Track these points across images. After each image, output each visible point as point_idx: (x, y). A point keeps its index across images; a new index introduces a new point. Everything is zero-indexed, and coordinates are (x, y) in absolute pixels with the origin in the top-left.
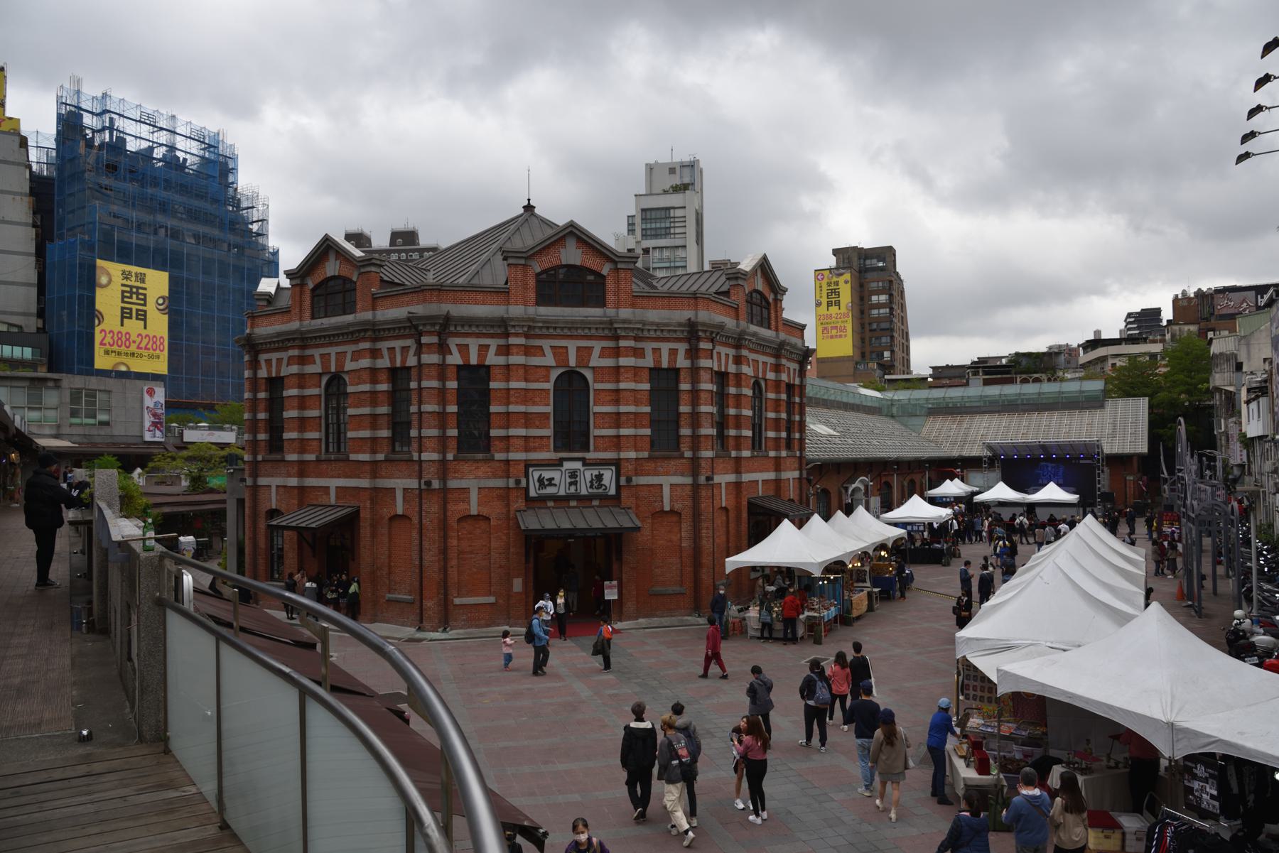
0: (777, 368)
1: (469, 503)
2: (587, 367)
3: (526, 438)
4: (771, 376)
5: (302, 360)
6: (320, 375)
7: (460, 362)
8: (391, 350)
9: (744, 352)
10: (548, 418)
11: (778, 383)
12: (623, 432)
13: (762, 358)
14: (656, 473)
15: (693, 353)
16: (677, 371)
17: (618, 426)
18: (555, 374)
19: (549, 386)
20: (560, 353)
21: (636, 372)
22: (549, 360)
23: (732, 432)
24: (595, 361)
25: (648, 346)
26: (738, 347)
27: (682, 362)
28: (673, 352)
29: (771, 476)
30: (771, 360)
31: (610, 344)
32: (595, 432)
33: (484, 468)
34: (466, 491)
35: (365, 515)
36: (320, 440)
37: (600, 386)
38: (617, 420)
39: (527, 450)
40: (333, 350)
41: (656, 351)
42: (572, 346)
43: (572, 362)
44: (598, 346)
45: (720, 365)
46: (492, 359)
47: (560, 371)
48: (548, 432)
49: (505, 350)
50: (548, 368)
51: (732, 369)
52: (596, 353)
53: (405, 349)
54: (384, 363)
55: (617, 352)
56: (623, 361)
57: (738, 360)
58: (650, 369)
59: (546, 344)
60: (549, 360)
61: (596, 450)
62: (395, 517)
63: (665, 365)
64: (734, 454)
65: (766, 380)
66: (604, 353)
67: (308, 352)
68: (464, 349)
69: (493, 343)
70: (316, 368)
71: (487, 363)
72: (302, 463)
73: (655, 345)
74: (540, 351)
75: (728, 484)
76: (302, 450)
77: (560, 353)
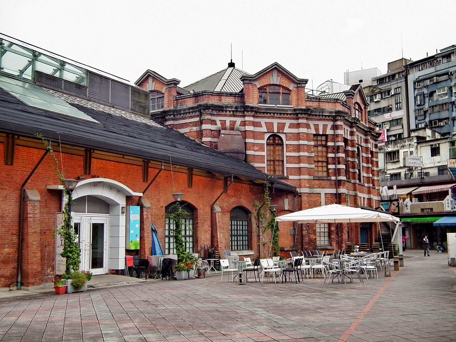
0: (366, 141)
2: (283, 133)
4: (363, 144)
9: (355, 130)
15: (335, 127)
16: (327, 136)
17: (299, 162)
18: (267, 136)
19: (264, 142)
20: (270, 126)
21: (307, 137)
22: (264, 129)
23: (351, 170)
24: (287, 130)
25: (311, 123)
26: (351, 127)
27: (329, 132)
28: (325, 127)
31: (295, 122)
37: (288, 142)
42: (275, 122)
44: (288, 122)
51: (349, 138)
55: (298, 126)
57: (352, 134)
58: (314, 135)
59: (263, 121)
60: (264, 129)
63: (321, 133)
64: (353, 181)
65: (362, 146)
66: (291, 126)
73: (316, 123)
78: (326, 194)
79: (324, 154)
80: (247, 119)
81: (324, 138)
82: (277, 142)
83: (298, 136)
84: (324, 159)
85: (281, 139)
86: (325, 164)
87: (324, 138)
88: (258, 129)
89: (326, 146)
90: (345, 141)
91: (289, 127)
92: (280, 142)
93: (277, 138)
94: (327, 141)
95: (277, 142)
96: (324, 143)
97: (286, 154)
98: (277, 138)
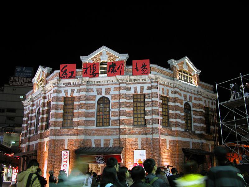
1: (64, 145)
2: (109, 94)
5: (33, 105)
7: (65, 96)
10: (94, 114)
13: (188, 95)
16: (144, 95)
18: (98, 97)
19: (95, 102)
20: (99, 92)
21: (126, 96)
24: (112, 92)
25: (132, 86)
29: (199, 141)
30: (193, 96)
34: (64, 141)
38: (120, 113)
40: (38, 100)
41: (136, 89)
44: (113, 87)
45: (163, 93)
46: (75, 94)
47: (100, 96)
48: (94, 119)
49: (79, 91)
50: (95, 96)
51: (171, 95)
52: (112, 90)
53: (51, 94)
54: (46, 101)
59: (94, 88)
60: (95, 93)
63: (139, 93)
66: (115, 89)
67: (34, 103)
68: (66, 92)
69: (76, 89)
74: (92, 90)
77: (99, 92)
79: (142, 108)
80: (81, 87)
81: (142, 97)
82: (106, 102)
83: (120, 96)
84: (143, 112)
86: (143, 116)
88: (91, 94)
91: (114, 91)
92: (108, 101)
93: (106, 99)
94: (144, 98)
97: (112, 110)
98: (106, 99)
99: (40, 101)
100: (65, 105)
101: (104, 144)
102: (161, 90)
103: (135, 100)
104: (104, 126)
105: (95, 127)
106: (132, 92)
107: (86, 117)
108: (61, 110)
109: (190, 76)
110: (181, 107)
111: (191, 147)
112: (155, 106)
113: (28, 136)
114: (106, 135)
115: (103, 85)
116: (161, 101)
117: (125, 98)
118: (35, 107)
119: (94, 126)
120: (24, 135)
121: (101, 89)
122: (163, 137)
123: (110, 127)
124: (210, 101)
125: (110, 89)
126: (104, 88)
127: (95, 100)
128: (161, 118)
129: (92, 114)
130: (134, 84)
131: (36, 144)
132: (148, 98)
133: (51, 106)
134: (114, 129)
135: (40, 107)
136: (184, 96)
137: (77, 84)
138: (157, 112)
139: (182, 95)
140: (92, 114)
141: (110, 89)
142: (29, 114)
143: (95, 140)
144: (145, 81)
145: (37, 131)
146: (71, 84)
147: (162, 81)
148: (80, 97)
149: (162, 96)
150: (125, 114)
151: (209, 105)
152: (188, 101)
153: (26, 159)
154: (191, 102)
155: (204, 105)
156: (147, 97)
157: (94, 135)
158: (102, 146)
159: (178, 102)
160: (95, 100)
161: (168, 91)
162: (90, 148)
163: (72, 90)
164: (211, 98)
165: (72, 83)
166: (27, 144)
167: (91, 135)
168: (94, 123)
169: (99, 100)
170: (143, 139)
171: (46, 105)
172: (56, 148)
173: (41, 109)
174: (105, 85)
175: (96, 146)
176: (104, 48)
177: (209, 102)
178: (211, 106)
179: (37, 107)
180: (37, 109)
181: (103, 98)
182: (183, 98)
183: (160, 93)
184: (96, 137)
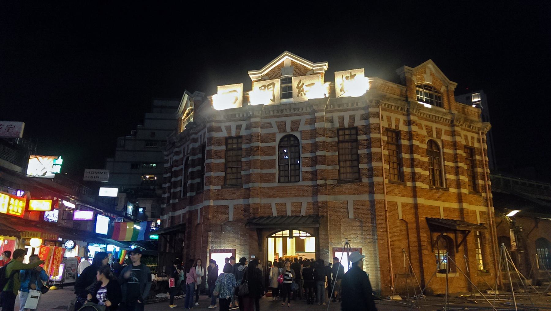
0: (453, 134)
2: (297, 130)
3: (261, 175)
4: (446, 138)
6: (183, 158)
7: (226, 135)
8: (201, 136)
9: (412, 118)
11: (455, 145)
12: (318, 167)
13: (434, 126)
14: (342, 193)
16: (356, 128)
18: (279, 137)
19: (276, 144)
24: (302, 128)
30: (445, 128)
32: (303, 169)
33: (238, 193)
35: (187, 225)
36: (181, 191)
38: (315, 161)
39: (262, 182)
40: (185, 145)
43: (288, 129)
45: (389, 125)
48: (276, 171)
50: (274, 134)
51: (403, 128)
53: (205, 133)
56: (317, 125)
57: (409, 123)
58: (338, 130)
60: (275, 130)
61: (304, 180)
62: (198, 224)
63: (346, 125)
64: (409, 184)
65: (442, 141)
70: (181, 156)
71: (240, 135)
72: (174, 204)
75: (403, 205)
76: (174, 198)
78: (355, 202)
85: (296, 138)
87: (353, 132)
89: (356, 140)
90: (397, 134)
92: (296, 142)
94: (357, 134)
95: (292, 142)
96: (354, 137)
97: (302, 155)
98: (292, 139)
99: (188, 146)
100: (227, 150)
101: (292, 212)
102: (385, 118)
103: (341, 138)
104: (291, 182)
105: (276, 184)
106: (337, 125)
107: (261, 169)
108: (220, 158)
109: (436, 94)
110: (423, 148)
111: (442, 216)
112: (376, 147)
113: (171, 202)
114: (295, 196)
115: (287, 116)
116: (386, 138)
117: (324, 136)
118: (181, 156)
119: (275, 182)
120: (166, 201)
121: (285, 122)
122: (389, 198)
123: (301, 183)
124: (476, 136)
125: (298, 122)
126: (288, 121)
127: (274, 141)
128: (386, 166)
129: (271, 164)
130: (339, 111)
131: (184, 215)
132: (363, 134)
133: (206, 152)
134: (308, 186)
135: (189, 155)
136: (427, 129)
137: (245, 116)
138: (379, 156)
139: (424, 127)
140: (271, 164)
141: (298, 122)
142: (172, 167)
143: (277, 205)
144: (357, 105)
145: (185, 194)
146: (235, 115)
147: (386, 106)
148: (251, 136)
149: (388, 130)
150: (324, 160)
151: (473, 143)
152: (435, 136)
153: (168, 240)
154: (440, 138)
155: (464, 142)
156: (361, 132)
157: (274, 197)
158: (289, 213)
159: (415, 140)
160: (274, 141)
161: (398, 120)
162: (269, 217)
163: (237, 126)
164: (477, 130)
165: (237, 116)
166: (170, 214)
167: (270, 197)
168: (275, 178)
169: (282, 140)
170: (357, 201)
171: (198, 151)
172: (215, 219)
173: (190, 158)
174: (291, 115)
175: (280, 214)
176: (286, 55)
177: (473, 138)
178: (476, 145)
179: (184, 156)
180: (185, 159)
181: (289, 137)
182: (424, 132)
183: (384, 124)
184: (278, 200)
